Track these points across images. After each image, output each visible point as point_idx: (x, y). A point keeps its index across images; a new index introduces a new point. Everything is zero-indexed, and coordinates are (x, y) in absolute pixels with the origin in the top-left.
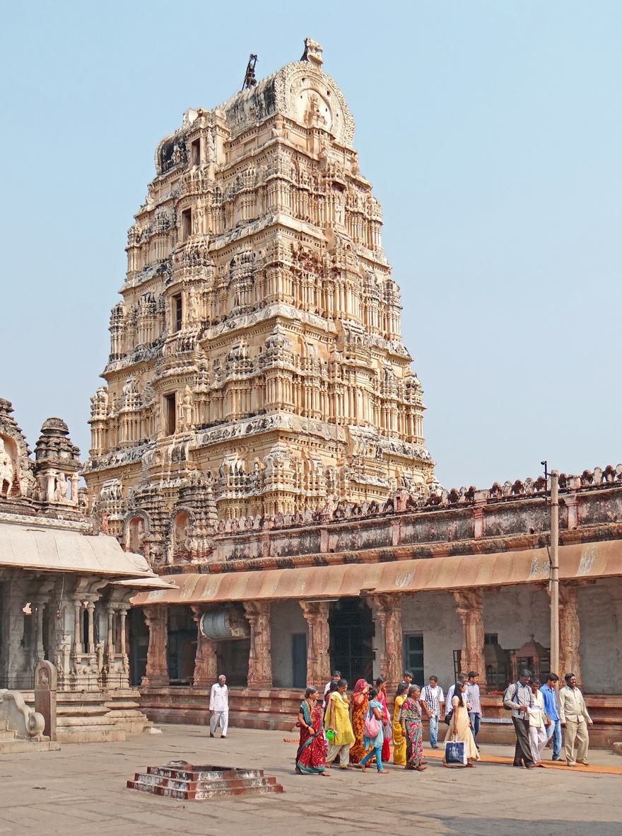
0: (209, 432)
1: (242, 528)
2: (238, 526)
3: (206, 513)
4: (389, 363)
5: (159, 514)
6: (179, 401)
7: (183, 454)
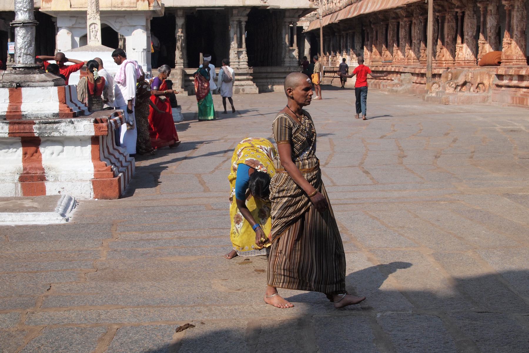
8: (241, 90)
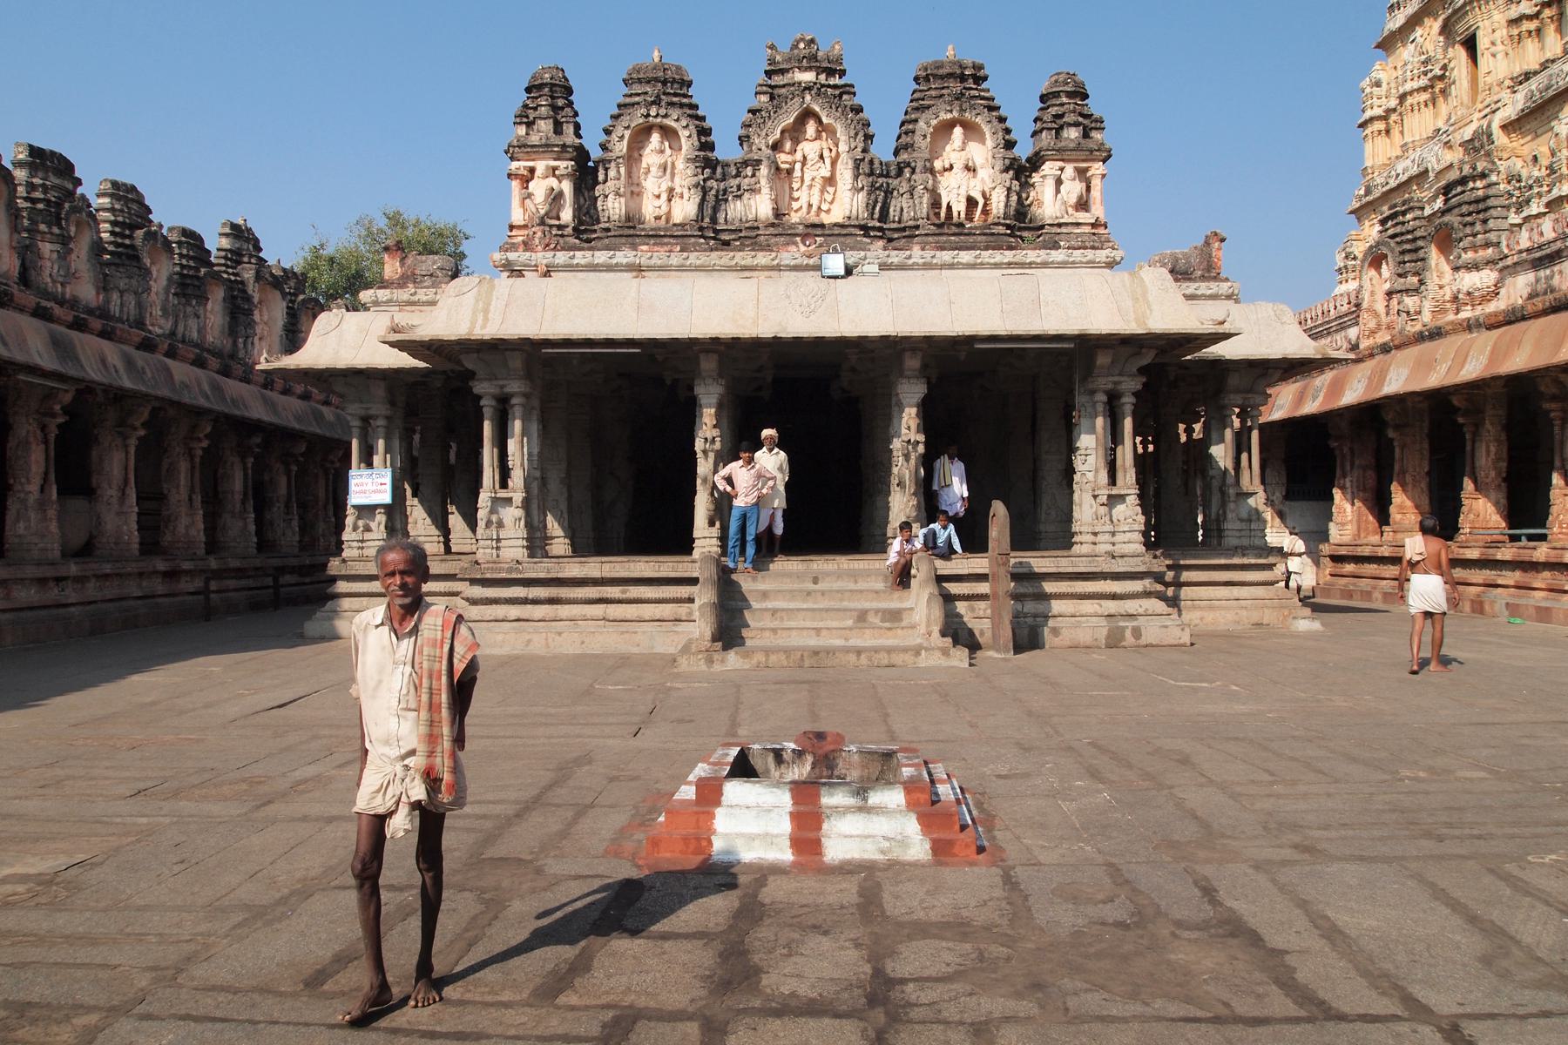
0: (1534, 84)
1: (1549, 235)
2: (1542, 234)
3: (1485, 221)
5: (1415, 240)
6: (1482, 43)
7: (1490, 135)
8: (1128, 633)
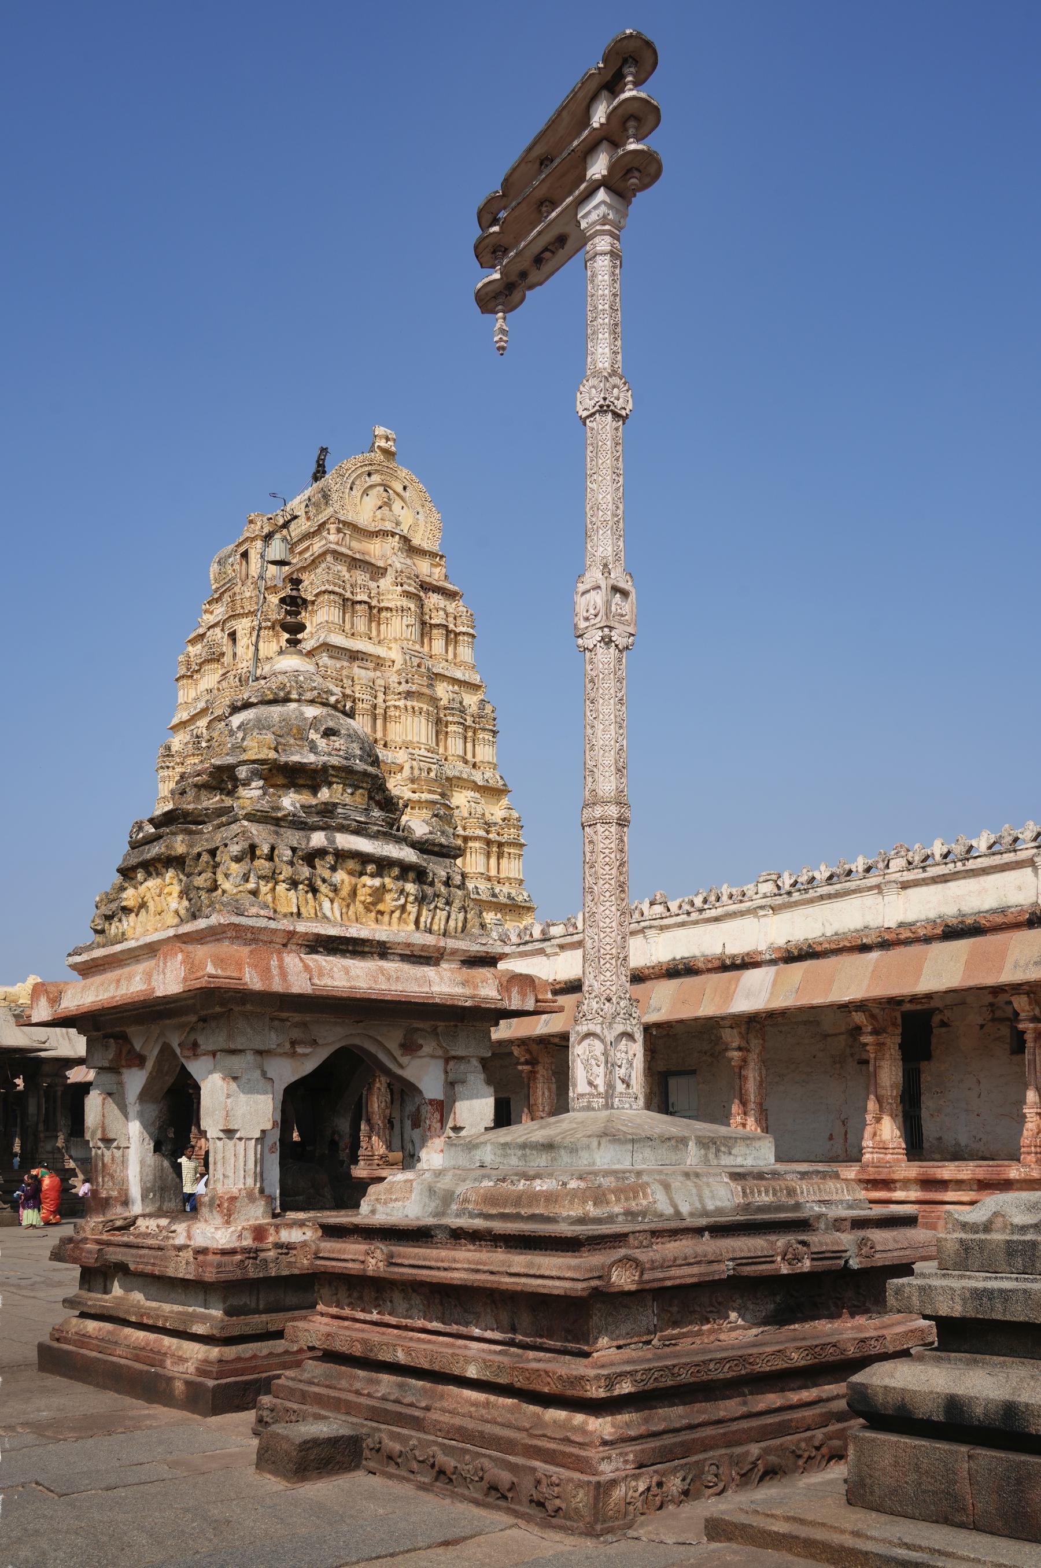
4: (477, 795)
